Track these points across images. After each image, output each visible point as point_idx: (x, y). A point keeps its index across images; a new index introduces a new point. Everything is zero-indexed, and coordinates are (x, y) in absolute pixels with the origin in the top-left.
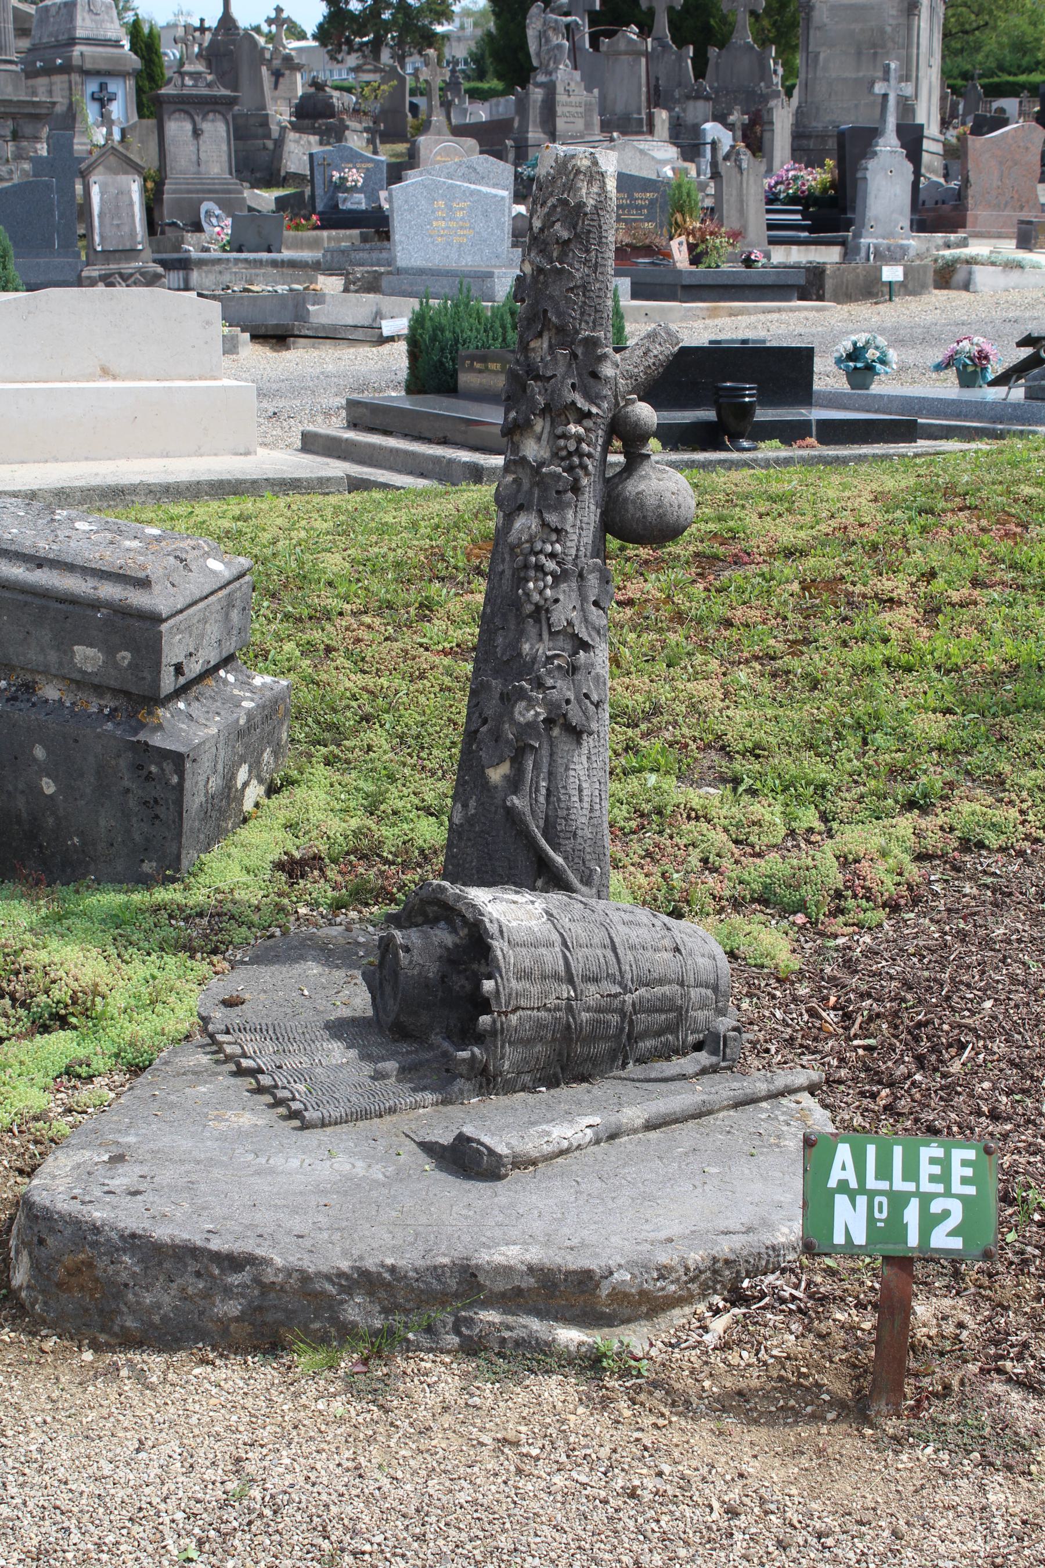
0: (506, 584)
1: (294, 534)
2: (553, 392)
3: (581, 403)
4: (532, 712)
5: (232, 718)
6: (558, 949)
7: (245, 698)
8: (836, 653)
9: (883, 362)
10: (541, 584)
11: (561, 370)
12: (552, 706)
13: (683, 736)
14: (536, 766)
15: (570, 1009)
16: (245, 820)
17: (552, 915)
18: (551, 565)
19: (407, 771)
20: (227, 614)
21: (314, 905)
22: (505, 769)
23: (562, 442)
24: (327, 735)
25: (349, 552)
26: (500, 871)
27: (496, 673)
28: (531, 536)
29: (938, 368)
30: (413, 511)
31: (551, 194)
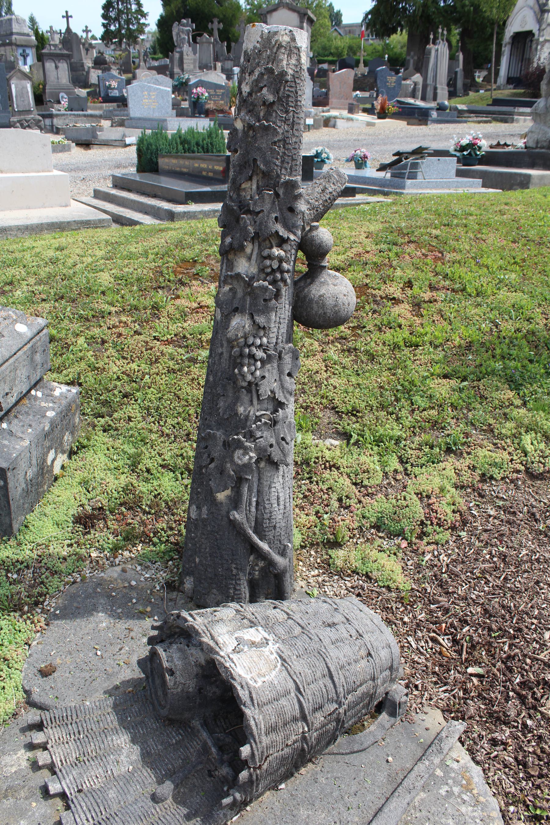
0: (225, 363)
1: (85, 259)
2: (261, 223)
3: (283, 232)
4: (247, 457)
5: (39, 429)
6: (293, 694)
7: (48, 409)
8: (376, 335)
9: (328, 159)
10: (253, 368)
11: (267, 207)
12: (260, 451)
13: (311, 403)
14: (250, 490)
15: (304, 738)
16: (56, 479)
17: (284, 660)
18: (260, 354)
19: (154, 436)
20: (32, 359)
21: (101, 549)
22: (228, 492)
23: (268, 262)
24: (104, 410)
25: (113, 271)
26: (226, 557)
27: (220, 424)
28: (245, 334)
29: (348, 160)
30: (145, 244)
31: (258, 65)
